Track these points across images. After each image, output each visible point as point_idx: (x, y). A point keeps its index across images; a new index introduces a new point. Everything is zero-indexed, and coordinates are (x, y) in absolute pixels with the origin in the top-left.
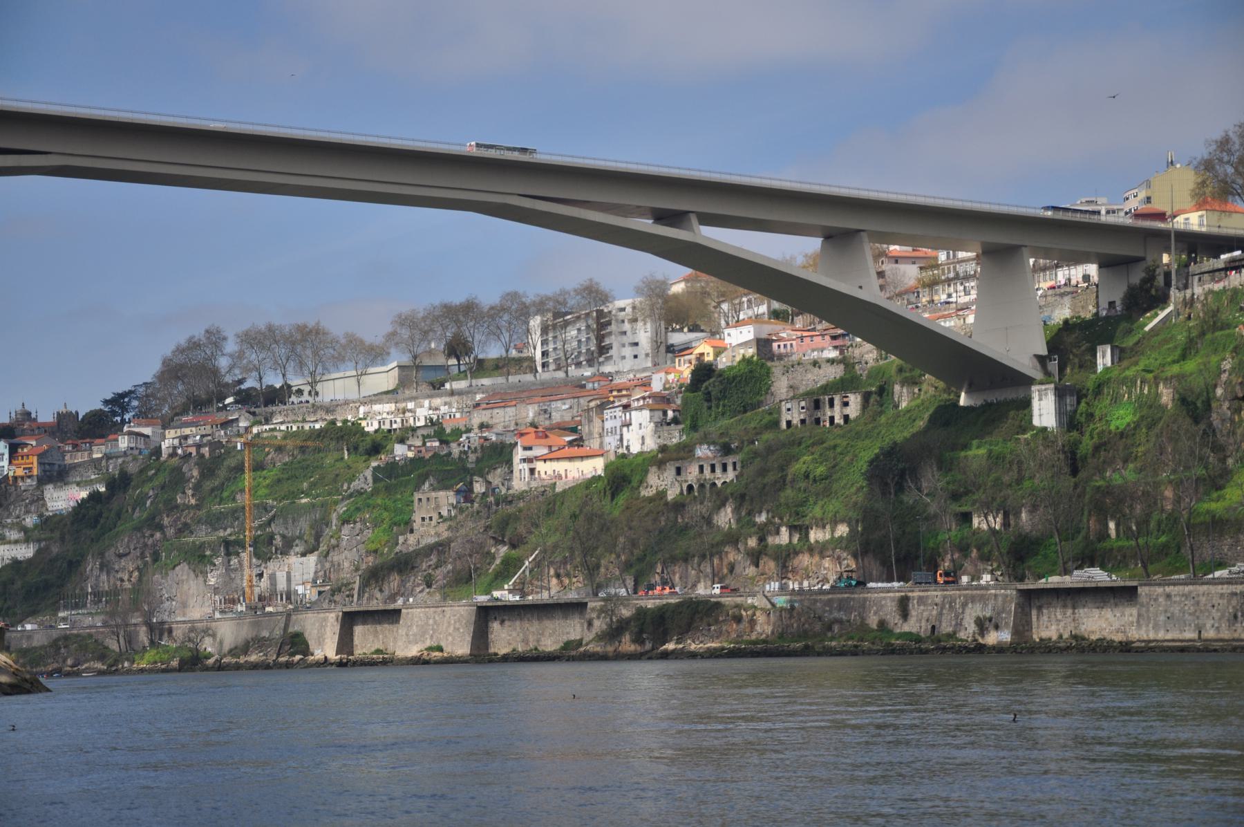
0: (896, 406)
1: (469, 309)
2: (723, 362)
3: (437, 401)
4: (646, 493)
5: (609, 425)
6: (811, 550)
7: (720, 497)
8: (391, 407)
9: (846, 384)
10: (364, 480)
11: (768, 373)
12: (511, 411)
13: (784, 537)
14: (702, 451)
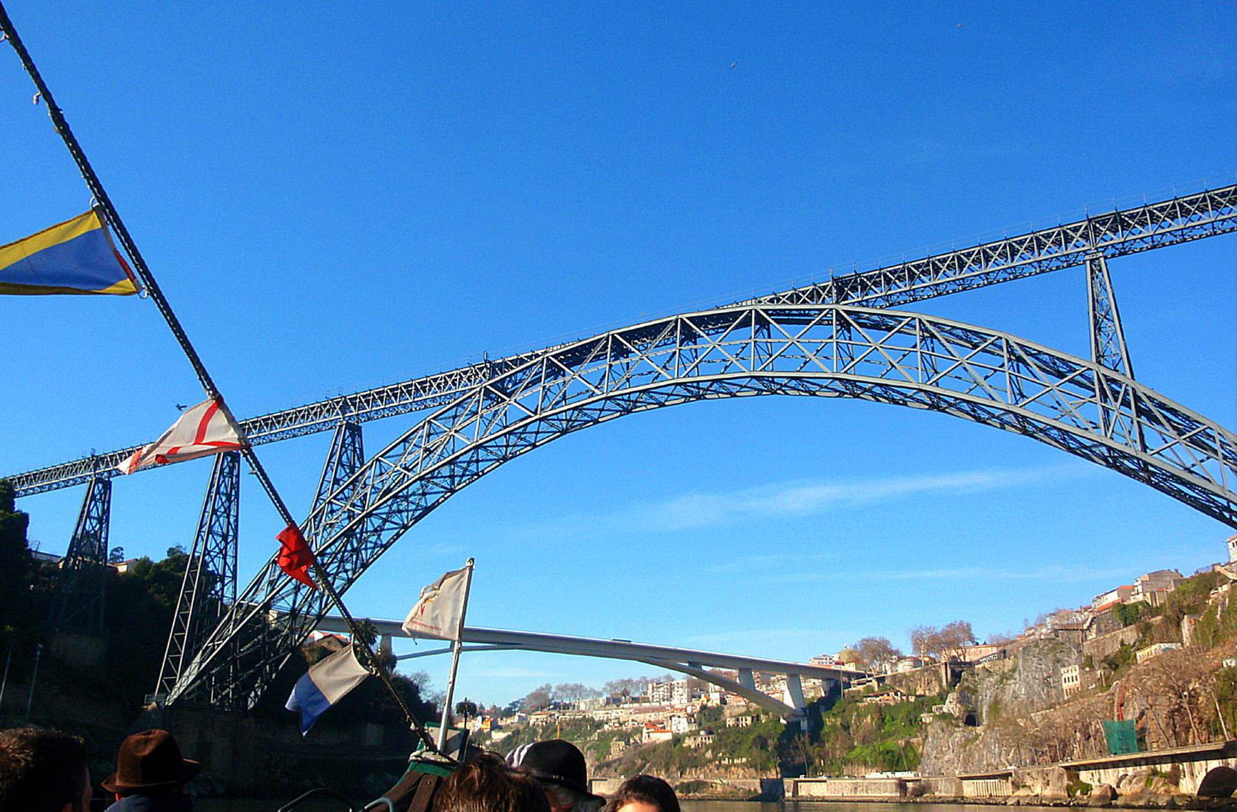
1: (630, 681)
2: (709, 704)
3: (618, 711)
5: (673, 723)
6: (735, 765)
8: (604, 712)
9: (747, 713)
10: (595, 737)
11: (723, 708)
12: (642, 715)
14: (702, 733)
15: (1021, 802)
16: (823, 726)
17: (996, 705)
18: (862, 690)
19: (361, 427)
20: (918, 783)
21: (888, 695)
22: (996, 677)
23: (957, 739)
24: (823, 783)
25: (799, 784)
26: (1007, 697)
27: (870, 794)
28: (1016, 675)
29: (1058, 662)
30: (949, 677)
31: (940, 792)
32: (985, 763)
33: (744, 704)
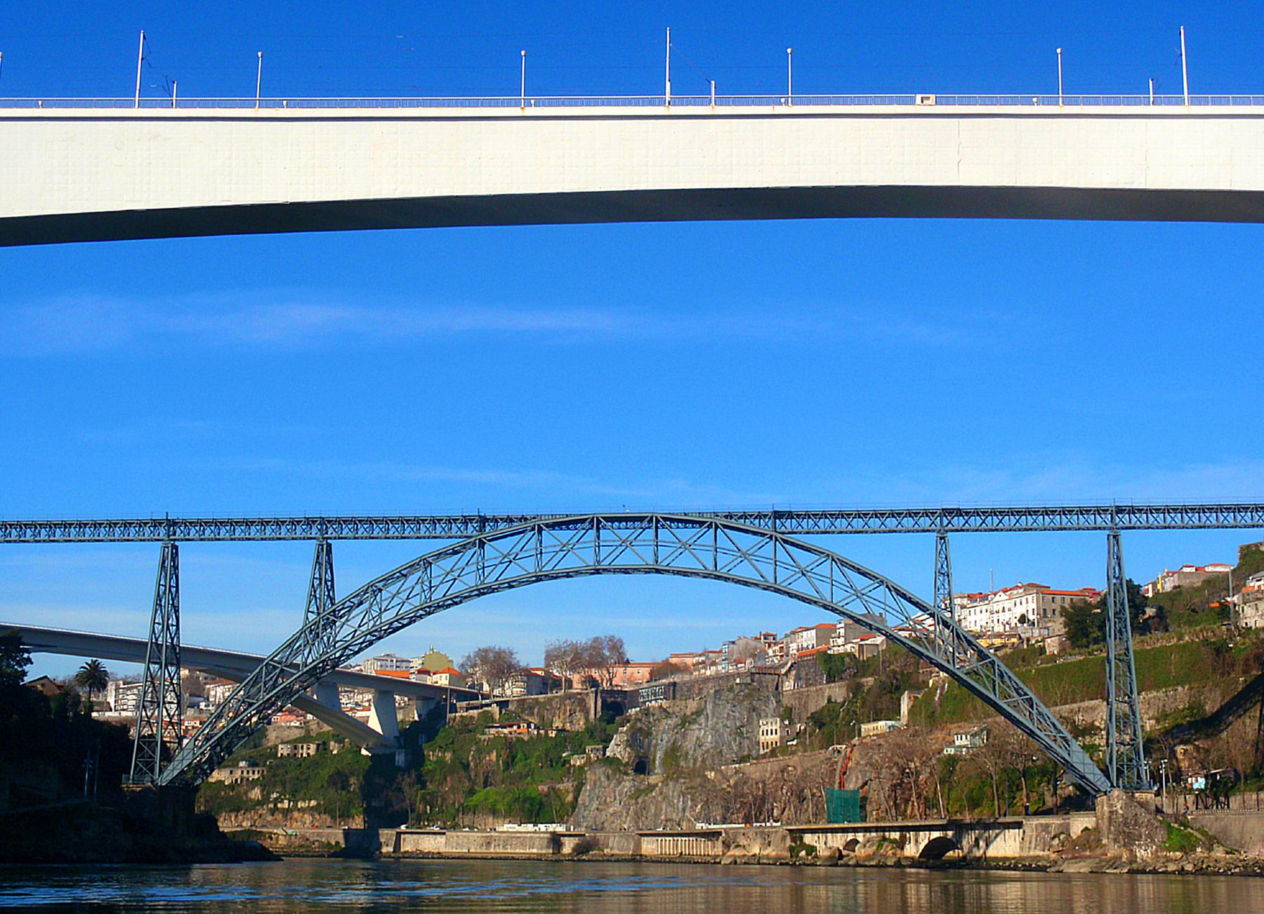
0: (332, 751)
4: (211, 780)
7: (254, 783)
9: (306, 739)
13: (286, 804)
14: (242, 764)
15: (738, 861)
16: (424, 762)
17: (673, 753)
18: (476, 715)
19: (331, 545)
20: (581, 838)
21: (519, 727)
22: (675, 720)
23: (625, 790)
24: (438, 836)
25: (402, 836)
26: (689, 744)
27: (509, 851)
28: (702, 720)
29: (754, 711)
30: (599, 708)
31: (612, 849)
32: (663, 817)
33: (298, 724)
